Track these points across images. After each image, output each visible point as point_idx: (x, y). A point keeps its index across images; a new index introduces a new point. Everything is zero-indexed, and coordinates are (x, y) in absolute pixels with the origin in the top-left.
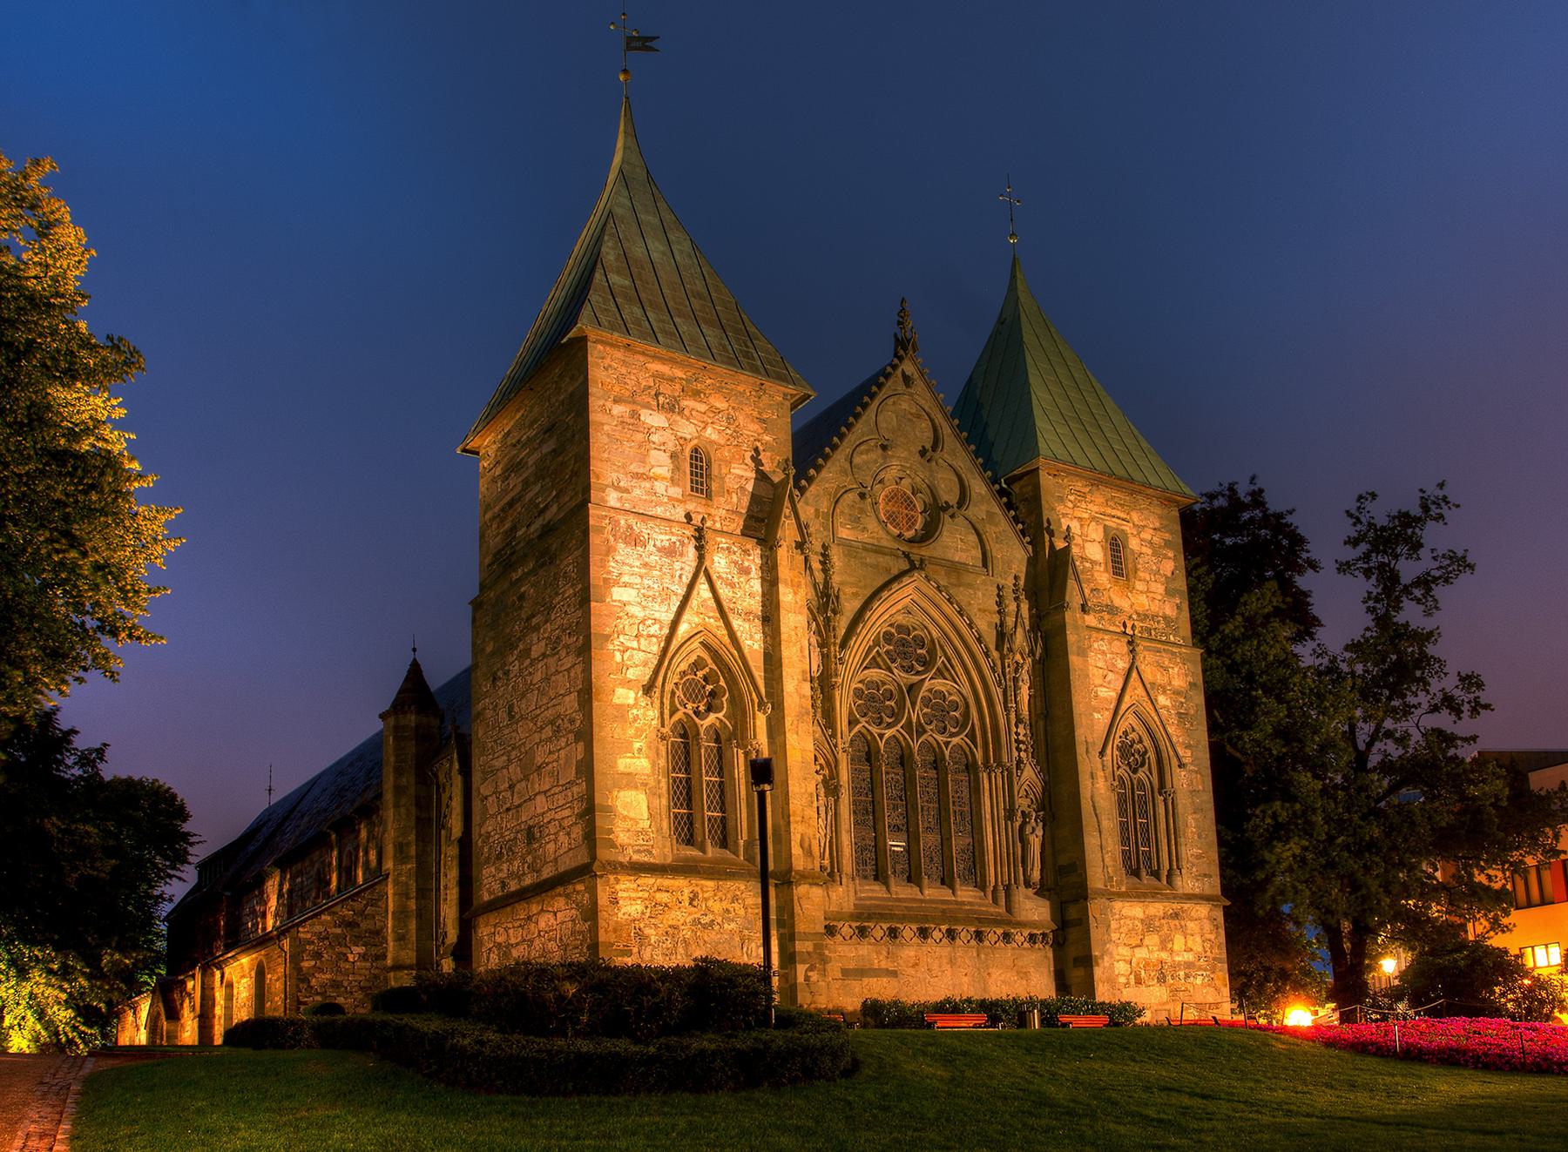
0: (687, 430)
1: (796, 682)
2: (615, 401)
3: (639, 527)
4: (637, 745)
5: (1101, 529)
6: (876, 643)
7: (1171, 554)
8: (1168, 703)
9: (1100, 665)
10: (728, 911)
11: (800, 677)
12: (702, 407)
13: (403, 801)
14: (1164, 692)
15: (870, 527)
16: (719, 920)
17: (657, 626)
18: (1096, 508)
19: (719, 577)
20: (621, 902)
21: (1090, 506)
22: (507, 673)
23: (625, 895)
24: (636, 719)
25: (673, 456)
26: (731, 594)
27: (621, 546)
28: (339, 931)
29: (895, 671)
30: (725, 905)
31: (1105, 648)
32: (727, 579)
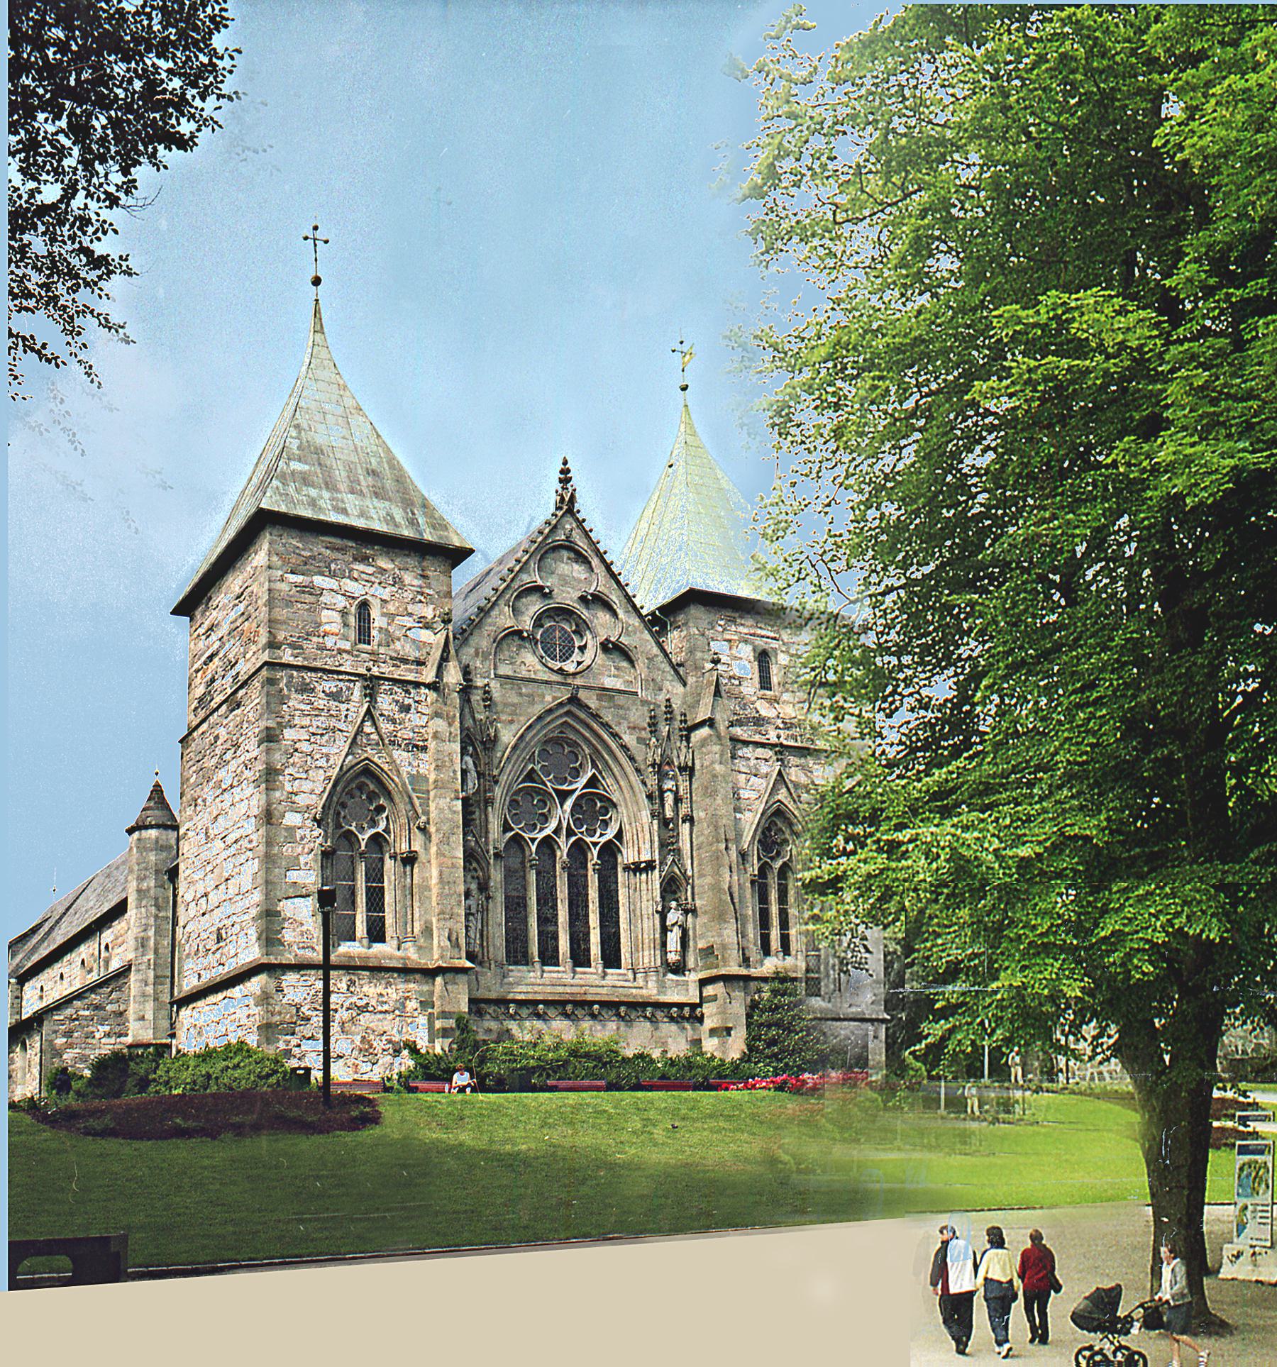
2: (292, 572)
3: (308, 676)
4: (302, 860)
5: (750, 648)
6: (532, 759)
9: (743, 770)
10: (381, 995)
12: (370, 570)
13: (144, 903)
16: (373, 1002)
18: (745, 630)
19: (381, 715)
21: (741, 629)
22: (204, 801)
24: (302, 839)
25: (344, 613)
27: (294, 695)
28: (87, 1013)
31: (749, 755)
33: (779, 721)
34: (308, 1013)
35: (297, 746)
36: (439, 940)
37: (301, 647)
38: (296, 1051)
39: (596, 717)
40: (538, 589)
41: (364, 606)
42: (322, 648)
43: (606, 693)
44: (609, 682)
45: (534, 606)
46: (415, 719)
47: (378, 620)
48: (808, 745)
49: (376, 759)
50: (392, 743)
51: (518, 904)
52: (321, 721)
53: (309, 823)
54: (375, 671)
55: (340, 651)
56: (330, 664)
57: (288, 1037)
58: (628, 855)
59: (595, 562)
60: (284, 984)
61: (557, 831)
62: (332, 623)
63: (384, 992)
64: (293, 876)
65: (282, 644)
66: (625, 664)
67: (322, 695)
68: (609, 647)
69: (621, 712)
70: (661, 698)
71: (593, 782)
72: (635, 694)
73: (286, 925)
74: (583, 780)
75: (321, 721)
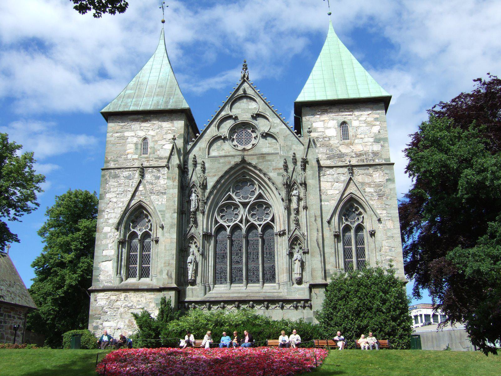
0: (142, 134)
1: (171, 214)
3: (117, 171)
4: (110, 245)
5: (335, 122)
7: (378, 123)
8: (372, 190)
10: (139, 301)
11: (173, 212)
14: (370, 187)
15: (225, 148)
17: (121, 204)
20: (98, 300)
23: (99, 297)
25: (136, 144)
26: (151, 187)
29: (237, 200)
30: (138, 299)
31: (333, 173)
32: (150, 182)
33: (353, 153)
34: (106, 310)
35: (111, 200)
36: (165, 276)
37: (117, 161)
38: (101, 326)
39: (255, 167)
40: (229, 117)
41: (145, 139)
42: (126, 159)
43: (263, 156)
44: (265, 150)
45: (229, 123)
46: (162, 182)
47: (150, 144)
48: (372, 163)
49: (144, 201)
50: (151, 193)
51: (224, 256)
52: (121, 189)
53: (114, 230)
54: (146, 164)
55: (133, 160)
56: (129, 165)
57: (98, 320)
58: (277, 228)
59: (258, 99)
60: (98, 297)
61: (241, 221)
62: (130, 148)
63: (140, 300)
64: (105, 253)
65: (110, 161)
66: (274, 141)
67: (123, 178)
68: (266, 135)
69: (269, 163)
70: (291, 154)
71: (260, 196)
72: (278, 154)
73: (101, 273)
74: (255, 196)
75: (121, 189)
